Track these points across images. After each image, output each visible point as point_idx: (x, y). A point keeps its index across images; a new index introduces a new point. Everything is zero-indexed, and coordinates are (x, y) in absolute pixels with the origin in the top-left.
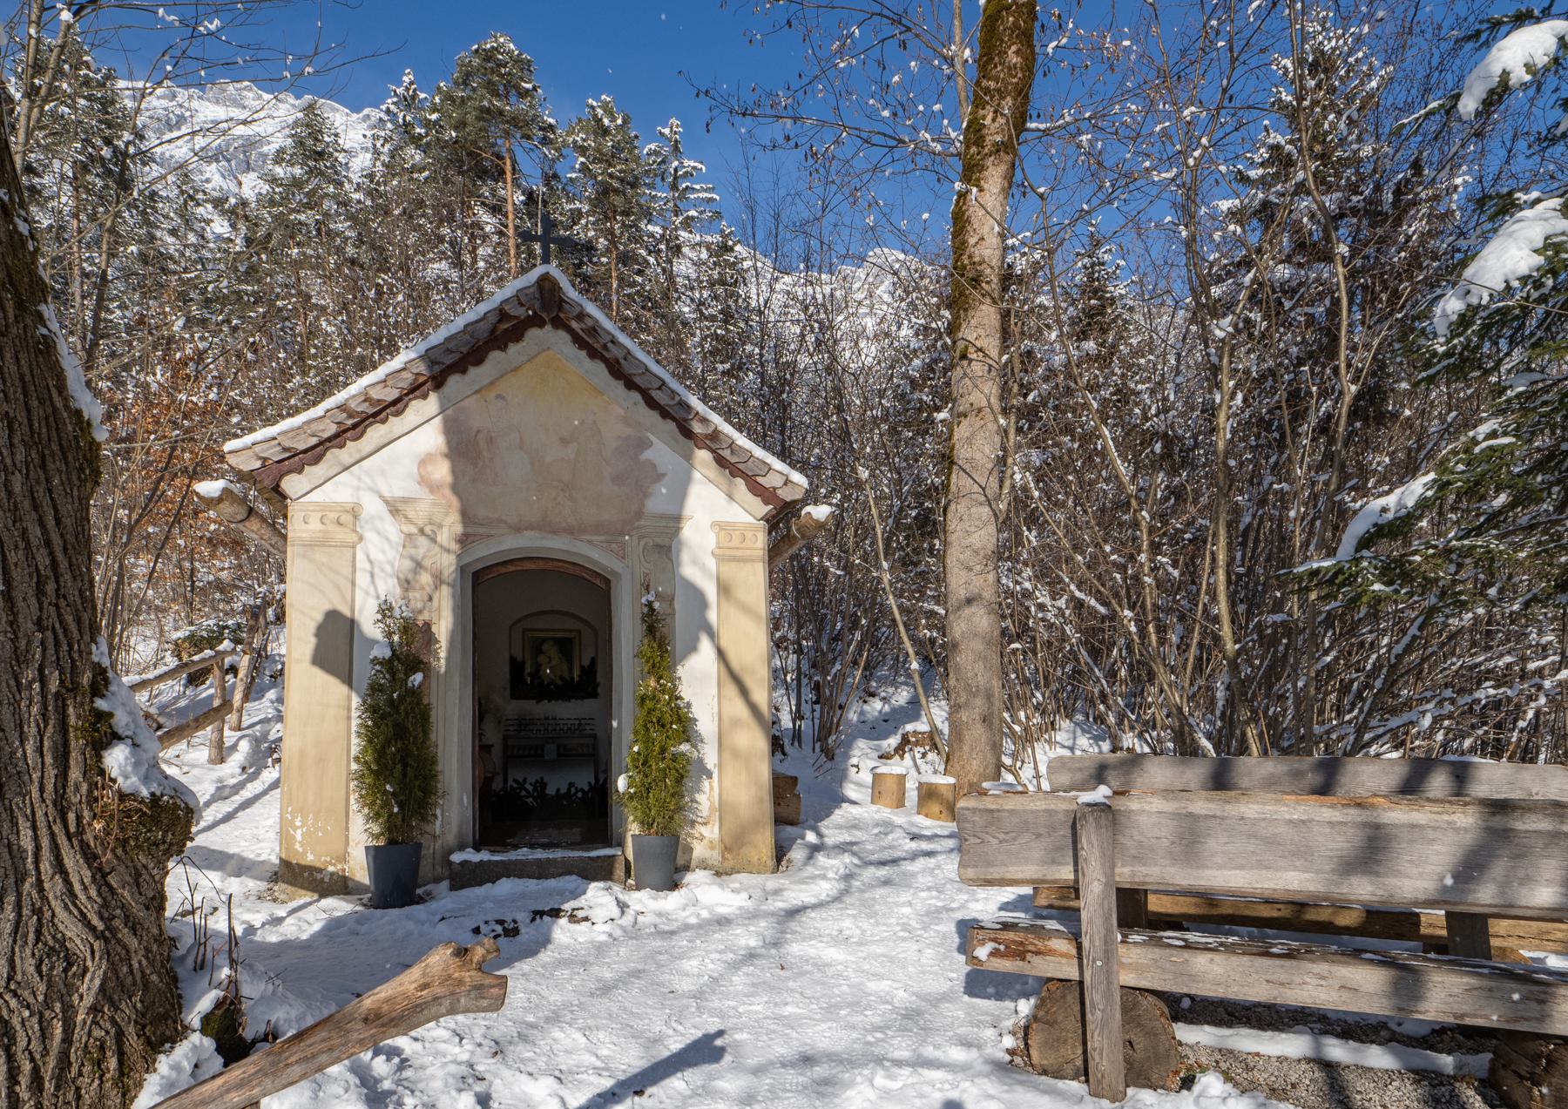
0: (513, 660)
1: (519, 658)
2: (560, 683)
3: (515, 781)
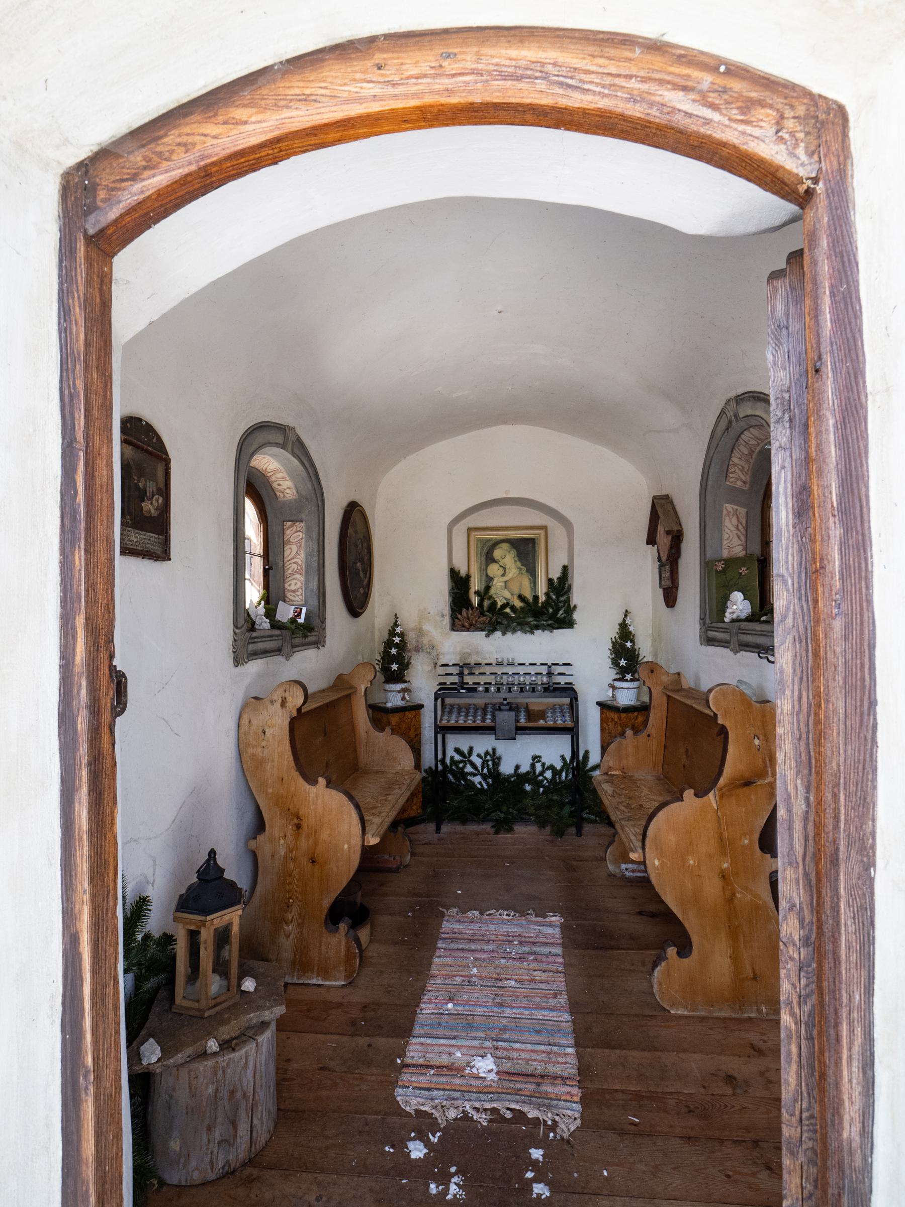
0: (454, 574)
1: (463, 573)
2: (518, 604)
3: (457, 750)
